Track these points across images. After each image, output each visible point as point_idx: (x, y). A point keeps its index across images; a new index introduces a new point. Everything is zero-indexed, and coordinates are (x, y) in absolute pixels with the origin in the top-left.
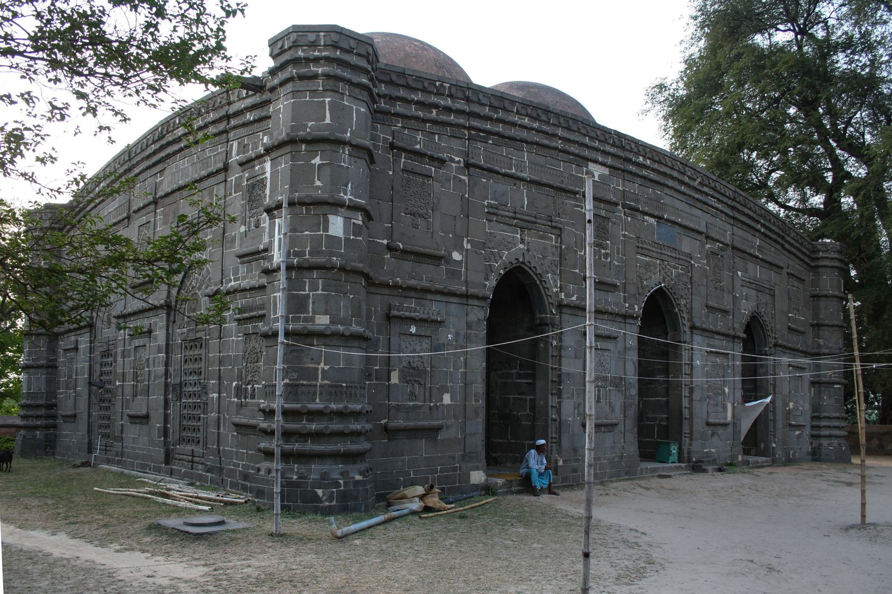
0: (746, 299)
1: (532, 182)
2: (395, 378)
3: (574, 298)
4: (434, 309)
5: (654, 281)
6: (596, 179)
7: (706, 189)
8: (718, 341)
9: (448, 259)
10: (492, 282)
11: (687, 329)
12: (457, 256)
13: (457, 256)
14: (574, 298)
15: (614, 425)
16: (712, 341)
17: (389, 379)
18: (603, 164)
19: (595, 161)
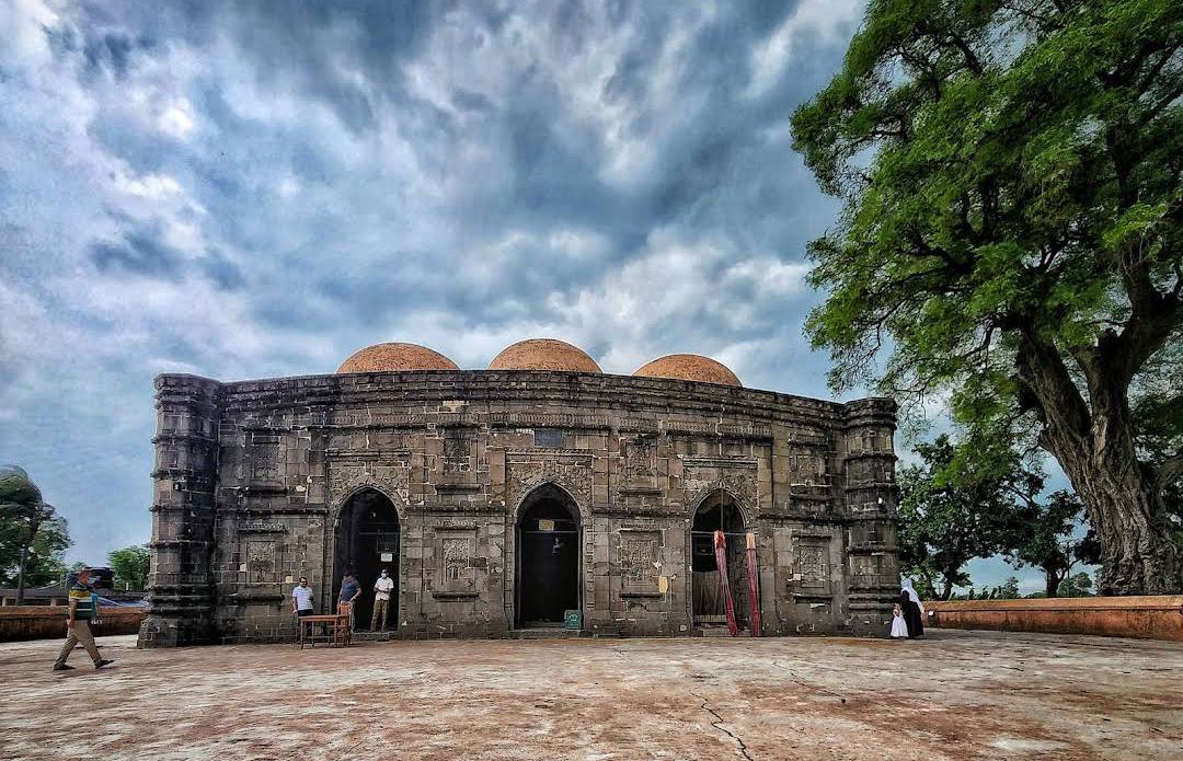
0: (699, 477)
1: (371, 428)
2: (243, 568)
3: (422, 503)
4: (277, 523)
5: (535, 480)
6: (454, 411)
7: (617, 390)
8: (639, 522)
9: (293, 491)
10: (336, 502)
11: (587, 514)
12: (300, 489)
13: (300, 489)
14: (422, 503)
15: (476, 596)
16: (628, 522)
17: (238, 568)
18: (459, 399)
19: (451, 399)
